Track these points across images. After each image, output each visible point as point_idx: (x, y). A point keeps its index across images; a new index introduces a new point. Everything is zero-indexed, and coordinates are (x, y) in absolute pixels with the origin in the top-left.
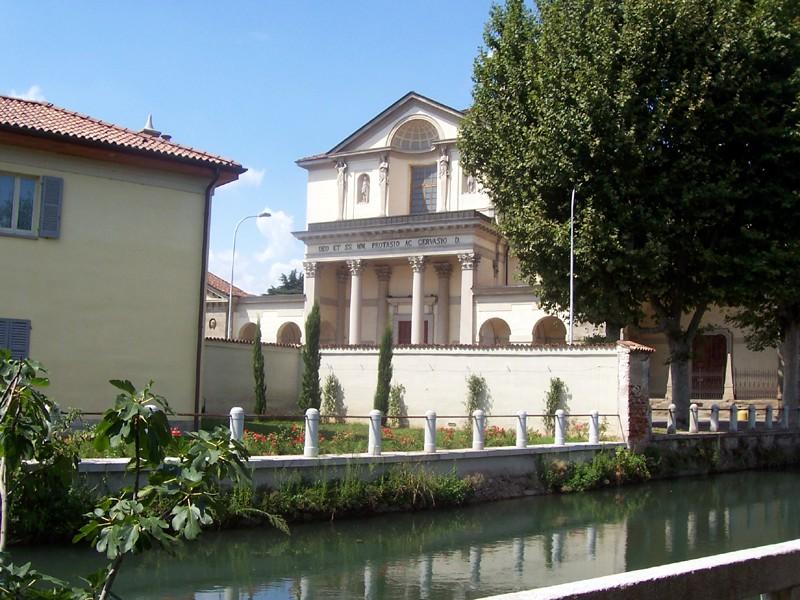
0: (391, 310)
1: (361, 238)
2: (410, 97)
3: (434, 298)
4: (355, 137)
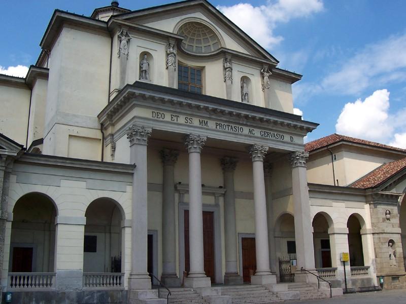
3: (222, 191)
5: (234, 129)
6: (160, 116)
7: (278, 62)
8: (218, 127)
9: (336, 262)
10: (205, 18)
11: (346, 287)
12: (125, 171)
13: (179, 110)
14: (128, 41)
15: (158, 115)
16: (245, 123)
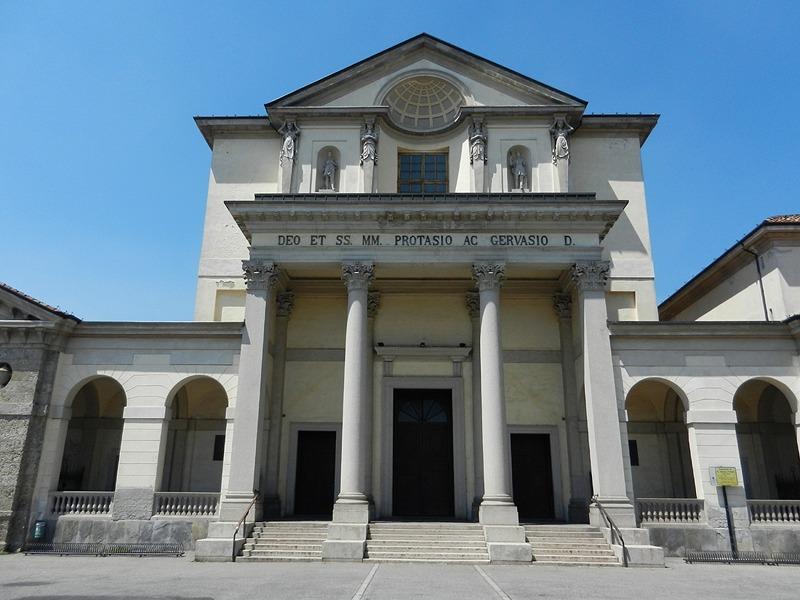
0: (379, 368)
2: (422, 40)
3: (466, 351)
4: (321, 86)
5: (432, 241)
7: (586, 103)
9: (705, 490)
10: (433, 66)
11: (734, 548)
12: (234, 333)
13: (322, 227)
14: (297, 138)
15: (288, 240)
16: (453, 228)
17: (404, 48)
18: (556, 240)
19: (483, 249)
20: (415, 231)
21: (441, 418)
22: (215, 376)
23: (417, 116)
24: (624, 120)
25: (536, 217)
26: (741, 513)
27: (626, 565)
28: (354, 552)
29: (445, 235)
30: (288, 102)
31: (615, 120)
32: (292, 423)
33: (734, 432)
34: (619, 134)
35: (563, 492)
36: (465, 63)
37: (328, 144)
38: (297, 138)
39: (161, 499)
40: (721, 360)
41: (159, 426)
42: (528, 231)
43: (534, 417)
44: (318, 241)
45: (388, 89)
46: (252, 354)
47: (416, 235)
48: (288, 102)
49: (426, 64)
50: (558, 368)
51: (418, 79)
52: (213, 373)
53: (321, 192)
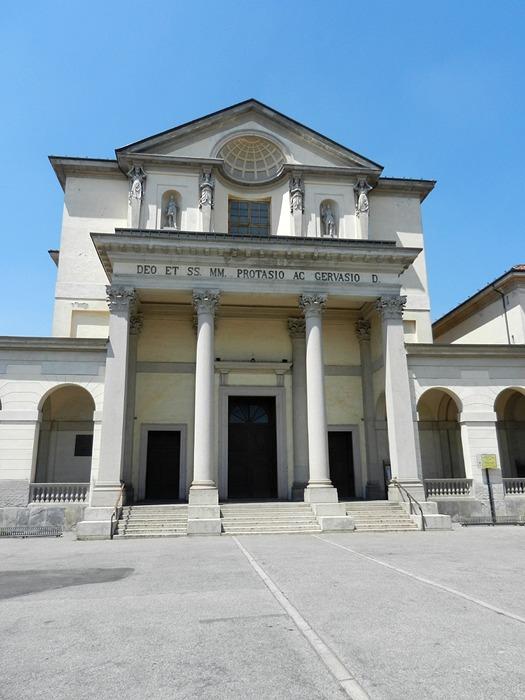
1: (222, 260)
2: (250, 105)
3: (287, 366)
4: (165, 138)
6: (149, 270)
7: (382, 168)
8: (241, 275)
9: (472, 471)
10: (260, 127)
11: (493, 514)
12: (99, 348)
13: (176, 260)
14: (144, 181)
17: (236, 110)
18: (366, 277)
19: (309, 283)
20: (255, 266)
21: (264, 420)
22: (83, 385)
23: (244, 169)
24: (410, 183)
25: (351, 259)
26: (498, 488)
27: (424, 529)
28: (214, 528)
29: (278, 270)
30: (136, 149)
31: (403, 183)
32: (142, 424)
33: (494, 428)
34: (405, 195)
35: (362, 475)
36: (286, 127)
37: (328, 197)
38: (144, 181)
39: (36, 490)
40: (486, 374)
41: (33, 428)
42: (344, 270)
43: (344, 419)
44: (172, 271)
45: (222, 145)
46: (116, 365)
47: (255, 269)
48: (136, 149)
49: (253, 126)
50: (358, 380)
51: (245, 137)
52: (81, 381)
53: (166, 229)
